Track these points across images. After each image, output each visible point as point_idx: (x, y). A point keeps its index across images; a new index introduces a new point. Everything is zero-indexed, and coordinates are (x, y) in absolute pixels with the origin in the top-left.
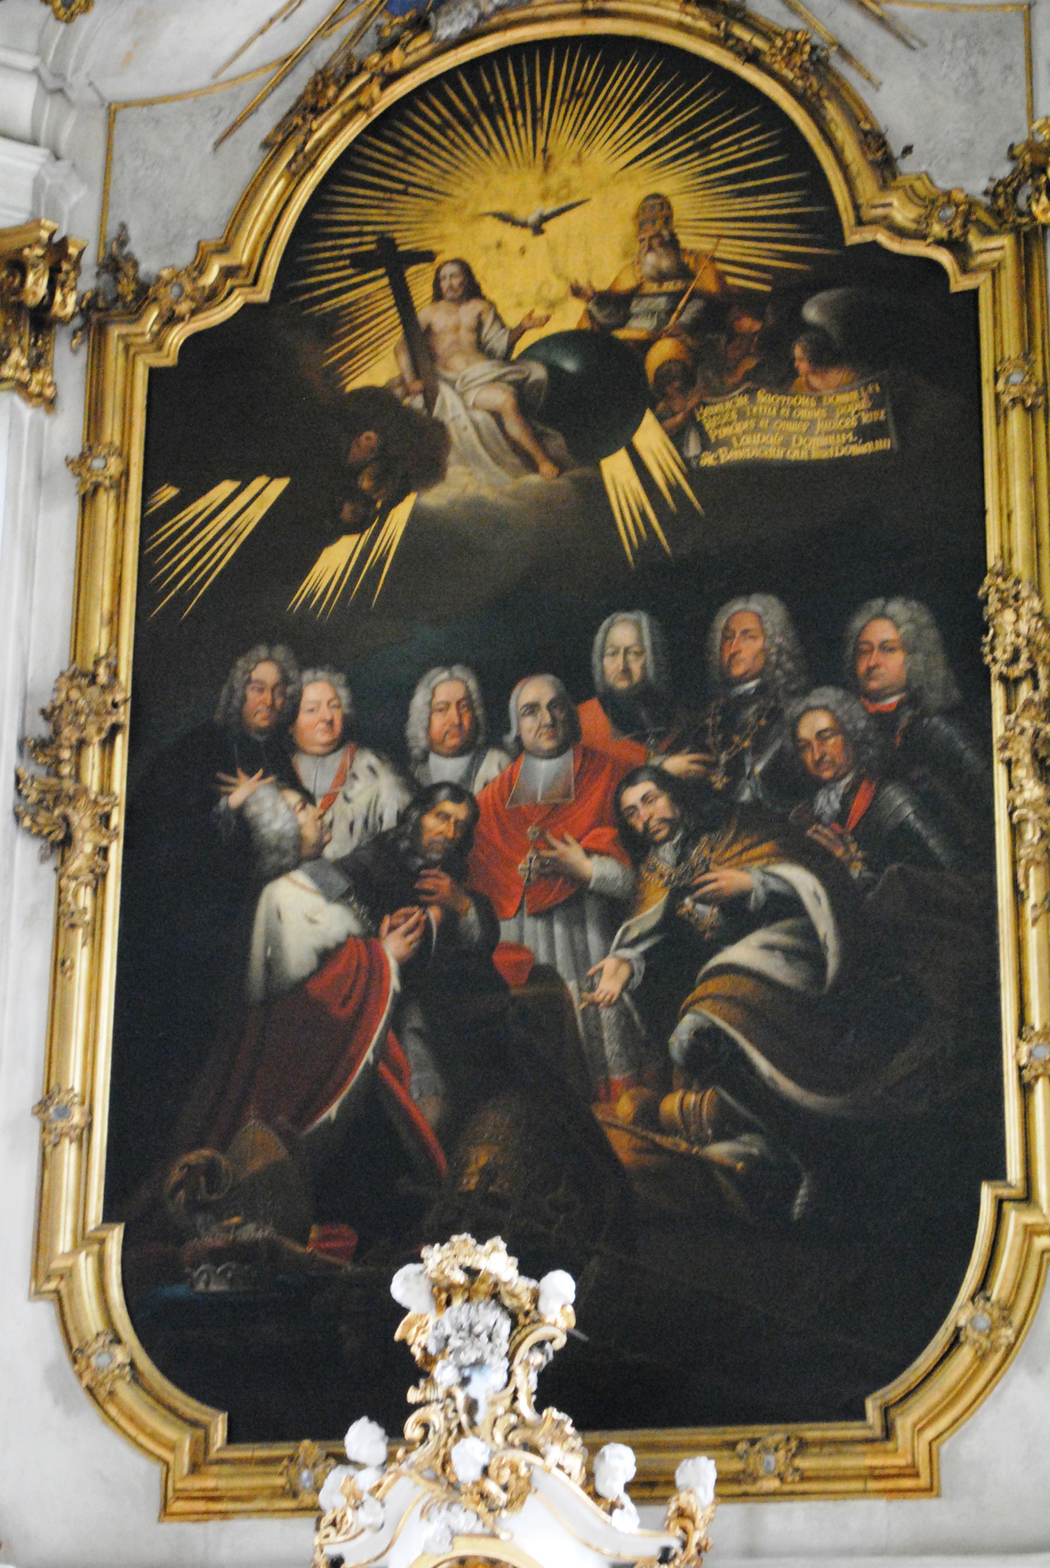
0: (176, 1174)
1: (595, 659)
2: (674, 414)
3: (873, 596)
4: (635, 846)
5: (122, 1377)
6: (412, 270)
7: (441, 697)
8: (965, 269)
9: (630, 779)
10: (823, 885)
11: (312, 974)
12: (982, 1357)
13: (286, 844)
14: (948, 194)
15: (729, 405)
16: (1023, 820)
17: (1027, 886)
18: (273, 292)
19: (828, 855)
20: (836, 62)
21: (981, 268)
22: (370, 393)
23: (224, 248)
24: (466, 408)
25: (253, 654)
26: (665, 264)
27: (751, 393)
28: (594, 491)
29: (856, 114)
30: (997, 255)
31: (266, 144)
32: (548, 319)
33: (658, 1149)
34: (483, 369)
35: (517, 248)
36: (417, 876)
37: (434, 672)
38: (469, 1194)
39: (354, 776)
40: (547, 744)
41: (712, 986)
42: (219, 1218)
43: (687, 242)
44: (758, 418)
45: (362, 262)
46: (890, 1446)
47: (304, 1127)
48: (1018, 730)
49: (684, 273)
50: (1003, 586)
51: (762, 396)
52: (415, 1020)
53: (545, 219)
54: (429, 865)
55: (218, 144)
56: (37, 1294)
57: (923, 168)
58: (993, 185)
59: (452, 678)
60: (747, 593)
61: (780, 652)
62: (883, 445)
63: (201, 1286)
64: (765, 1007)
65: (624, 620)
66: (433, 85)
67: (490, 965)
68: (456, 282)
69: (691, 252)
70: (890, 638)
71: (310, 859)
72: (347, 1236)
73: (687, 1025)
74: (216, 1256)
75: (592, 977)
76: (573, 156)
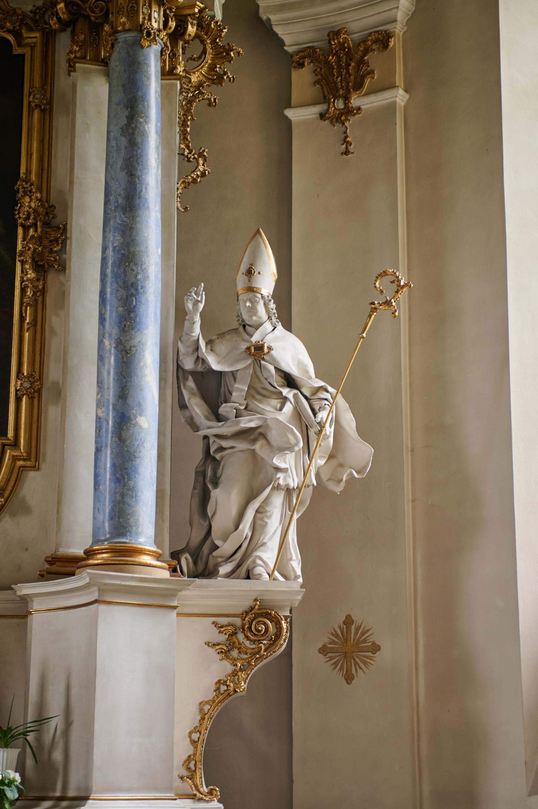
8: (20, 45)
14: (14, 10)
16: (26, 287)
17: (26, 315)
48: (27, 248)
50: (25, 186)
58: (34, 8)
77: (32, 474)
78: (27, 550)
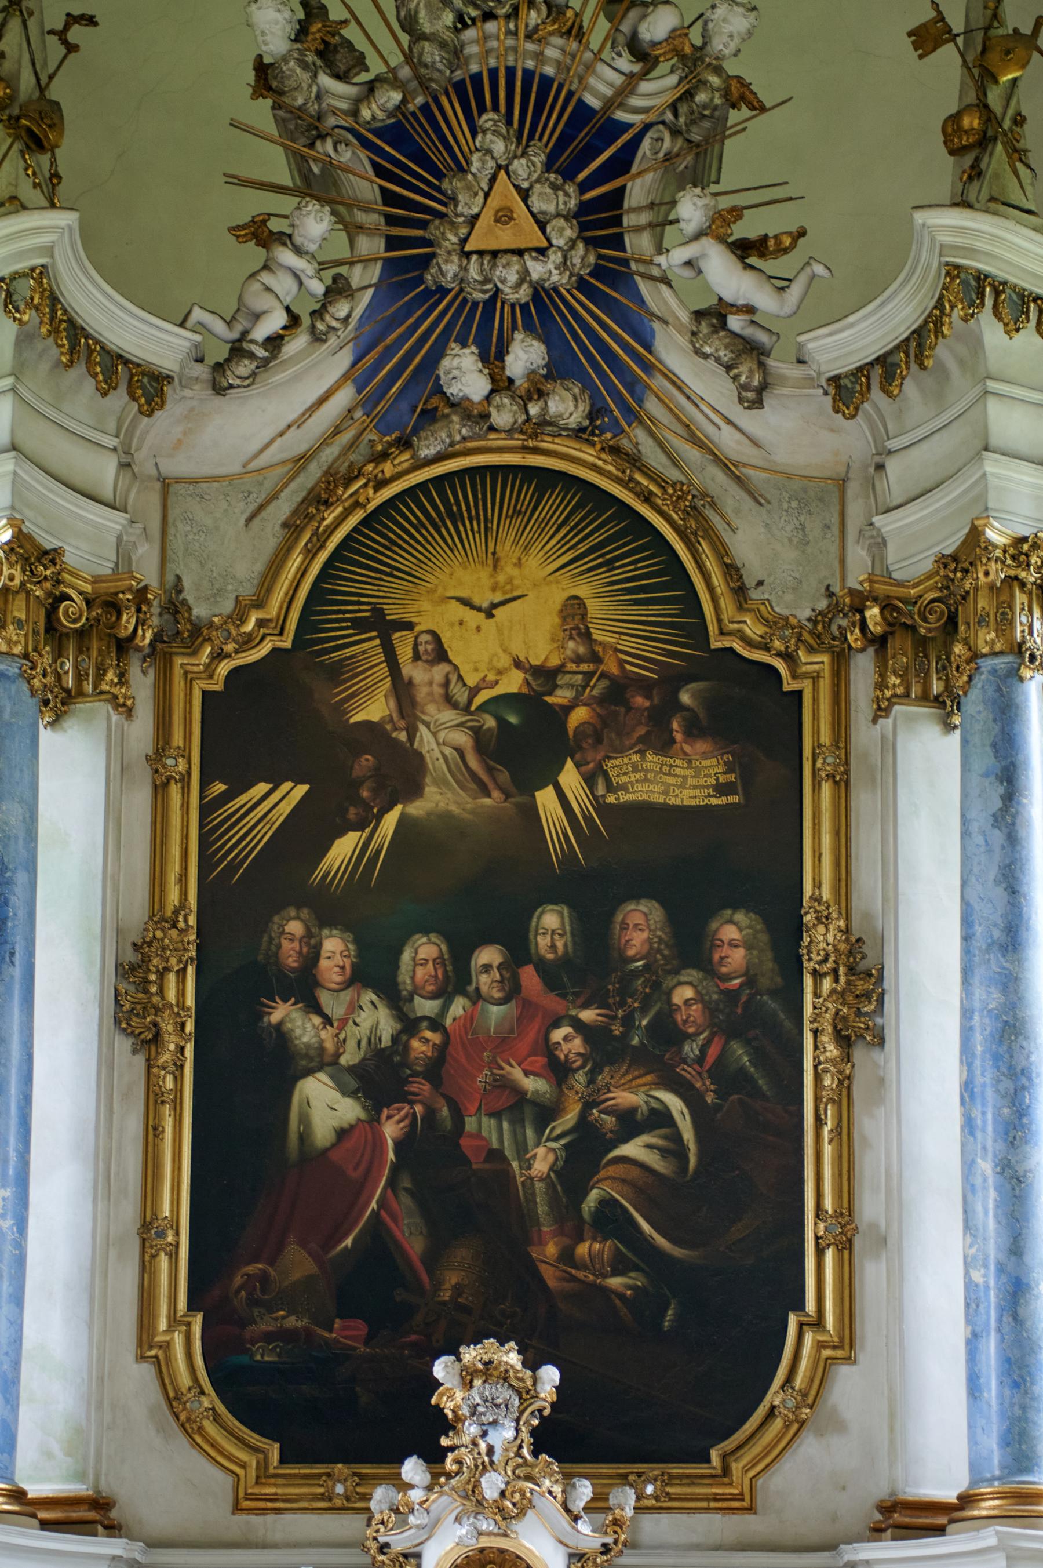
0: (238, 1280)
1: (531, 937)
2: (588, 763)
3: (725, 907)
4: (559, 1070)
5: (208, 1418)
6: (397, 635)
7: (422, 955)
8: (794, 676)
9: (556, 1025)
10: (688, 1106)
11: (333, 1146)
12: (787, 1427)
13: (312, 1053)
14: (786, 619)
15: (626, 760)
18: (294, 642)
19: (692, 1086)
20: (709, 512)
21: (805, 676)
22: (368, 724)
23: (259, 604)
24: (438, 744)
25: (284, 913)
26: (581, 650)
27: (642, 753)
28: (531, 813)
29: (721, 551)
30: (816, 667)
31: (285, 525)
32: (497, 682)
33: (574, 1279)
34: (449, 716)
35: (474, 626)
36: (406, 1081)
37: (417, 936)
38: (444, 1303)
39: (361, 1008)
40: (497, 995)
41: (611, 1171)
42: (271, 1311)
43: (597, 635)
44: (647, 771)
45: (362, 626)
46: (726, 1480)
47: (327, 1253)
49: (596, 659)
51: (650, 756)
52: (406, 1183)
53: (495, 606)
54: (415, 1074)
55: (249, 520)
56: (141, 1358)
57: (766, 596)
59: (430, 942)
60: (637, 897)
61: (661, 940)
62: (734, 799)
63: (258, 1357)
64: (649, 1188)
65: (552, 910)
66: (410, 492)
67: (458, 1145)
68: (429, 647)
69: (600, 644)
70: (735, 938)
71: (330, 1064)
72: (361, 1328)
73: (594, 1195)
74: (268, 1337)
75: (528, 1160)
76: (515, 561)
77: (844, 1371)
78: (844, 1488)
